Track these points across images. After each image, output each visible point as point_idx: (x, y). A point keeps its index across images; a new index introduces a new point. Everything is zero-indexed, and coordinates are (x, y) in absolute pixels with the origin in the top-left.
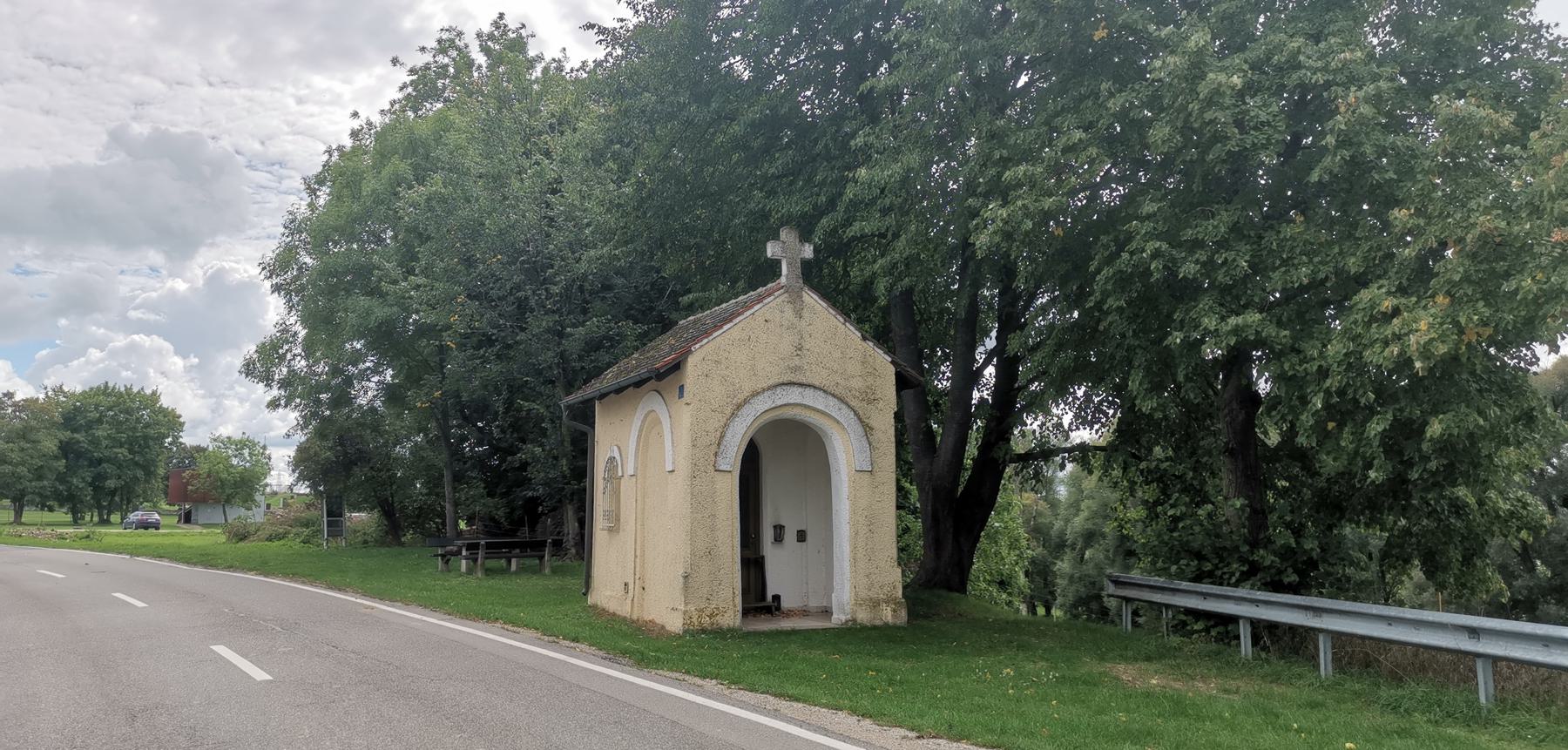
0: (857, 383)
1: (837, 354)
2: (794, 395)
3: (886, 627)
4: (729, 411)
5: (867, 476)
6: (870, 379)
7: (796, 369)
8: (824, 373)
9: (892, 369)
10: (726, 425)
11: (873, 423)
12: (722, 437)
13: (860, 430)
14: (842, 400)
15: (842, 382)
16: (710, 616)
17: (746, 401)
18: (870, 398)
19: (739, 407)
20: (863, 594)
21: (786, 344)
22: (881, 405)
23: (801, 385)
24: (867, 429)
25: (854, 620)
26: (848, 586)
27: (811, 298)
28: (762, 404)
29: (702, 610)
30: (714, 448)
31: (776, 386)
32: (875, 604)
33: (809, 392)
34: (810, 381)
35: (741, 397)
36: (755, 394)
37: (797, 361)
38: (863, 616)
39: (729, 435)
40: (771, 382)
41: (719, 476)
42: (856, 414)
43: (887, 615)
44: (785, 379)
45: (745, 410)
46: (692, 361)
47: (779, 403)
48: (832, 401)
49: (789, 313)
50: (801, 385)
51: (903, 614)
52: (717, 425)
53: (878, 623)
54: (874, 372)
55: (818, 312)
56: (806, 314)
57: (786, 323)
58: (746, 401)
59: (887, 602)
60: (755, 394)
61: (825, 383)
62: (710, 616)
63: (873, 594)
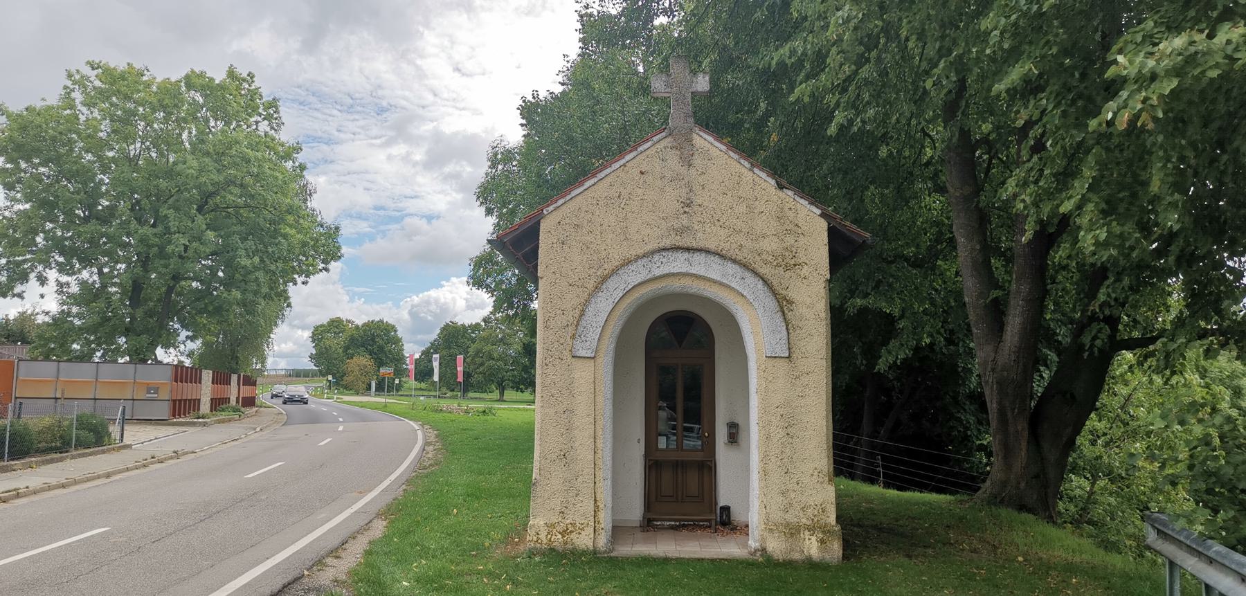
0: (771, 245)
1: (742, 209)
2: (678, 263)
3: (812, 565)
4: (591, 285)
5: (783, 363)
6: (790, 240)
7: (683, 230)
8: (723, 233)
9: (823, 225)
10: (587, 302)
11: (792, 295)
12: (582, 314)
13: (772, 304)
14: (745, 266)
15: (748, 244)
16: (563, 533)
17: (614, 272)
18: (789, 262)
19: (605, 279)
20: (777, 516)
21: (670, 199)
22: (805, 271)
23: (688, 249)
24: (783, 304)
25: (764, 550)
27: (704, 141)
28: (634, 275)
29: (553, 526)
30: (571, 329)
31: (653, 252)
32: (793, 531)
33: (698, 258)
34: (702, 244)
35: (608, 267)
37: (684, 220)
38: (777, 547)
39: (590, 312)
40: (649, 248)
42: (765, 282)
43: (812, 547)
44: (667, 243)
45: (611, 283)
46: (544, 226)
47: (657, 273)
48: (731, 268)
49: (673, 159)
50: (687, 249)
51: (836, 548)
52: (575, 302)
53: (796, 556)
54: (795, 230)
56: (697, 160)
57: (669, 174)
58: (614, 272)
59: (812, 529)
60: (627, 262)
61: (724, 246)
62: (563, 533)
63: (790, 517)
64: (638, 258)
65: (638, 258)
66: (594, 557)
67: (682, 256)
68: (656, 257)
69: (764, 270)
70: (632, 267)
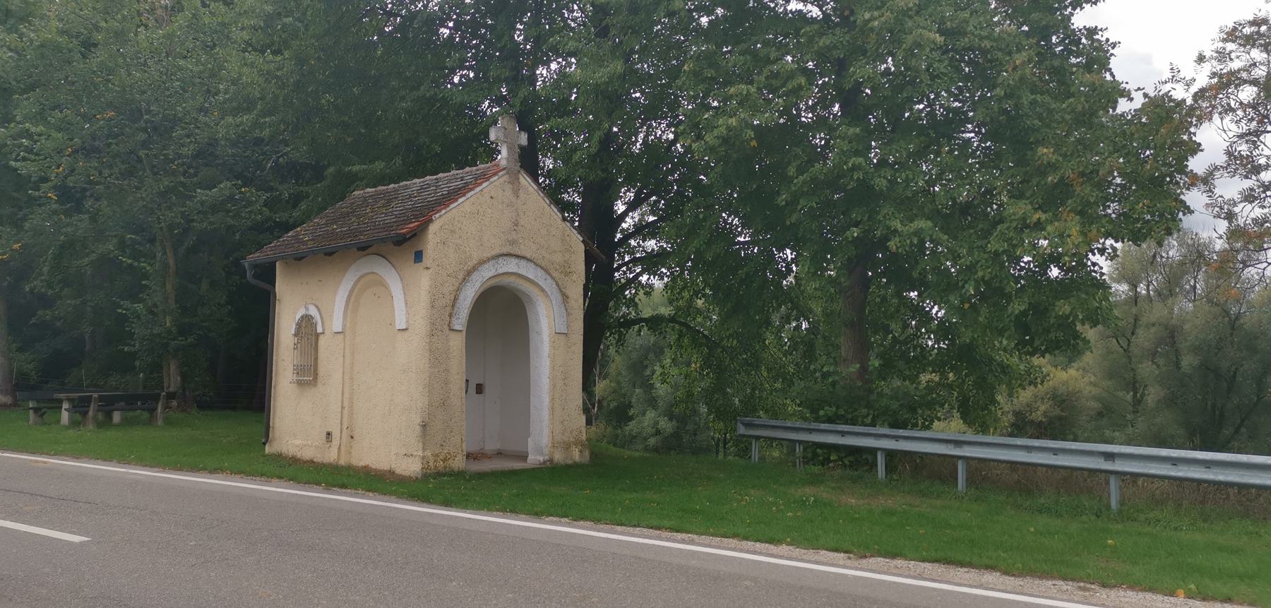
0: (558, 258)
2: (511, 266)
4: (461, 277)
7: (513, 243)
9: (583, 247)
10: (459, 290)
11: (568, 292)
12: (455, 299)
13: (560, 297)
19: (469, 273)
23: (517, 256)
24: (565, 297)
25: (551, 460)
26: (546, 432)
29: (437, 455)
30: (449, 309)
32: (567, 446)
33: (523, 263)
34: (524, 253)
35: (471, 264)
36: (482, 262)
38: (558, 457)
39: (461, 298)
41: (452, 335)
43: (576, 455)
44: (505, 250)
45: (475, 276)
46: (433, 228)
47: (501, 271)
48: (540, 272)
50: (517, 256)
53: (570, 462)
55: (531, 193)
58: (474, 269)
59: (576, 445)
60: (482, 262)
62: (444, 460)
64: (489, 260)
65: (489, 260)
66: (459, 475)
67: (514, 261)
68: (501, 260)
69: (555, 274)
70: (486, 266)
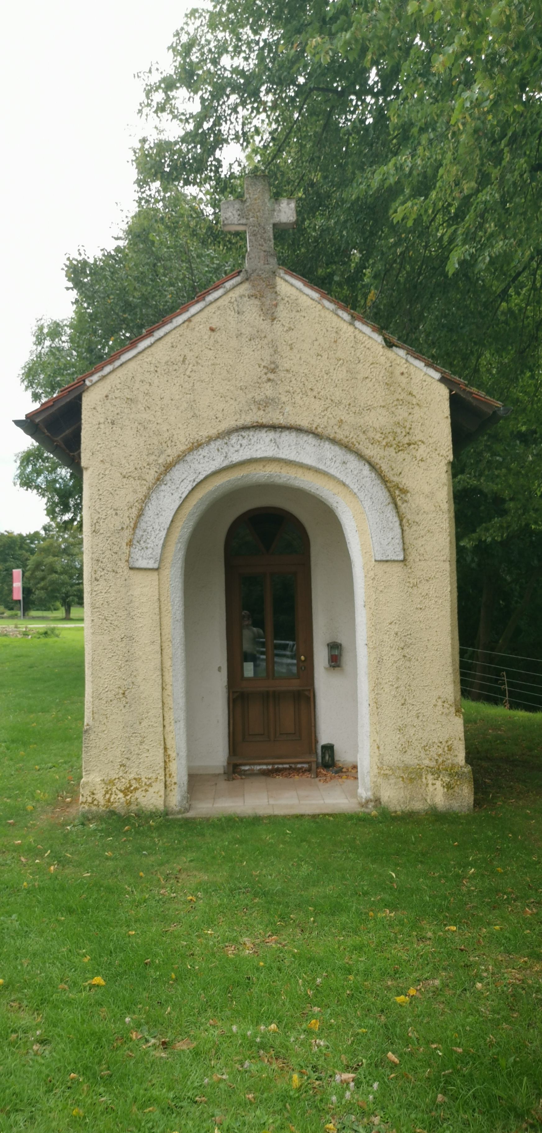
0: (378, 419)
2: (262, 445)
3: (437, 816)
4: (151, 476)
5: (397, 568)
6: (402, 413)
7: (265, 404)
8: (317, 406)
9: (443, 393)
10: (147, 498)
11: (406, 482)
12: (141, 514)
13: (381, 494)
14: (348, 447)
16: (126, 792)
17: (180, 459)
18: (402, 441)
19: (168, 467)
20: (393, 758)
22: (422, 451)
23: (273, 427)
24: (396, 494)
25: (377, 801)
27: (291, 288)
29: (112, 782)
30: (127, 534)
31: (230, 432)
32: (412, 776)
33: (288, 438)
34: (292, 420)
35: (172, 453)
36: (196, 446)
37: (268, 390)
38: (393, 796)
39: (150, 512)
40: (224, 426)
41: (138, 577)
42: (373, 467)
43: (436, 794)
44: (248, 419)
45: (177, 473)
46: (88, 401)
47: (236, 458)
48: (329, 450)
49: (252, 311)
50: (273, 427)
51: (466, 794)
52: (131, 498)
53: (418, 806)
56: (282, 312)
57: (247, 331)
58: (180, 459)
59: (436, 772)
60: (196, 446)
61: (319, 423)
62: (126, 792)
63: (410, 759)
64: (210, 440)
65: (210, 440)
66: (164, 821)
67: (266, 436)
68: (234, 438)
69: (369, 451)
70: (203, 452)
